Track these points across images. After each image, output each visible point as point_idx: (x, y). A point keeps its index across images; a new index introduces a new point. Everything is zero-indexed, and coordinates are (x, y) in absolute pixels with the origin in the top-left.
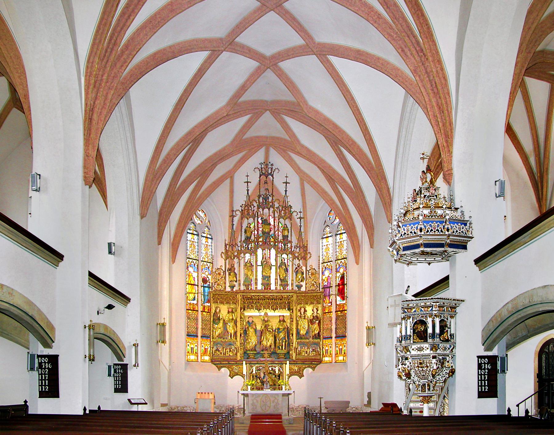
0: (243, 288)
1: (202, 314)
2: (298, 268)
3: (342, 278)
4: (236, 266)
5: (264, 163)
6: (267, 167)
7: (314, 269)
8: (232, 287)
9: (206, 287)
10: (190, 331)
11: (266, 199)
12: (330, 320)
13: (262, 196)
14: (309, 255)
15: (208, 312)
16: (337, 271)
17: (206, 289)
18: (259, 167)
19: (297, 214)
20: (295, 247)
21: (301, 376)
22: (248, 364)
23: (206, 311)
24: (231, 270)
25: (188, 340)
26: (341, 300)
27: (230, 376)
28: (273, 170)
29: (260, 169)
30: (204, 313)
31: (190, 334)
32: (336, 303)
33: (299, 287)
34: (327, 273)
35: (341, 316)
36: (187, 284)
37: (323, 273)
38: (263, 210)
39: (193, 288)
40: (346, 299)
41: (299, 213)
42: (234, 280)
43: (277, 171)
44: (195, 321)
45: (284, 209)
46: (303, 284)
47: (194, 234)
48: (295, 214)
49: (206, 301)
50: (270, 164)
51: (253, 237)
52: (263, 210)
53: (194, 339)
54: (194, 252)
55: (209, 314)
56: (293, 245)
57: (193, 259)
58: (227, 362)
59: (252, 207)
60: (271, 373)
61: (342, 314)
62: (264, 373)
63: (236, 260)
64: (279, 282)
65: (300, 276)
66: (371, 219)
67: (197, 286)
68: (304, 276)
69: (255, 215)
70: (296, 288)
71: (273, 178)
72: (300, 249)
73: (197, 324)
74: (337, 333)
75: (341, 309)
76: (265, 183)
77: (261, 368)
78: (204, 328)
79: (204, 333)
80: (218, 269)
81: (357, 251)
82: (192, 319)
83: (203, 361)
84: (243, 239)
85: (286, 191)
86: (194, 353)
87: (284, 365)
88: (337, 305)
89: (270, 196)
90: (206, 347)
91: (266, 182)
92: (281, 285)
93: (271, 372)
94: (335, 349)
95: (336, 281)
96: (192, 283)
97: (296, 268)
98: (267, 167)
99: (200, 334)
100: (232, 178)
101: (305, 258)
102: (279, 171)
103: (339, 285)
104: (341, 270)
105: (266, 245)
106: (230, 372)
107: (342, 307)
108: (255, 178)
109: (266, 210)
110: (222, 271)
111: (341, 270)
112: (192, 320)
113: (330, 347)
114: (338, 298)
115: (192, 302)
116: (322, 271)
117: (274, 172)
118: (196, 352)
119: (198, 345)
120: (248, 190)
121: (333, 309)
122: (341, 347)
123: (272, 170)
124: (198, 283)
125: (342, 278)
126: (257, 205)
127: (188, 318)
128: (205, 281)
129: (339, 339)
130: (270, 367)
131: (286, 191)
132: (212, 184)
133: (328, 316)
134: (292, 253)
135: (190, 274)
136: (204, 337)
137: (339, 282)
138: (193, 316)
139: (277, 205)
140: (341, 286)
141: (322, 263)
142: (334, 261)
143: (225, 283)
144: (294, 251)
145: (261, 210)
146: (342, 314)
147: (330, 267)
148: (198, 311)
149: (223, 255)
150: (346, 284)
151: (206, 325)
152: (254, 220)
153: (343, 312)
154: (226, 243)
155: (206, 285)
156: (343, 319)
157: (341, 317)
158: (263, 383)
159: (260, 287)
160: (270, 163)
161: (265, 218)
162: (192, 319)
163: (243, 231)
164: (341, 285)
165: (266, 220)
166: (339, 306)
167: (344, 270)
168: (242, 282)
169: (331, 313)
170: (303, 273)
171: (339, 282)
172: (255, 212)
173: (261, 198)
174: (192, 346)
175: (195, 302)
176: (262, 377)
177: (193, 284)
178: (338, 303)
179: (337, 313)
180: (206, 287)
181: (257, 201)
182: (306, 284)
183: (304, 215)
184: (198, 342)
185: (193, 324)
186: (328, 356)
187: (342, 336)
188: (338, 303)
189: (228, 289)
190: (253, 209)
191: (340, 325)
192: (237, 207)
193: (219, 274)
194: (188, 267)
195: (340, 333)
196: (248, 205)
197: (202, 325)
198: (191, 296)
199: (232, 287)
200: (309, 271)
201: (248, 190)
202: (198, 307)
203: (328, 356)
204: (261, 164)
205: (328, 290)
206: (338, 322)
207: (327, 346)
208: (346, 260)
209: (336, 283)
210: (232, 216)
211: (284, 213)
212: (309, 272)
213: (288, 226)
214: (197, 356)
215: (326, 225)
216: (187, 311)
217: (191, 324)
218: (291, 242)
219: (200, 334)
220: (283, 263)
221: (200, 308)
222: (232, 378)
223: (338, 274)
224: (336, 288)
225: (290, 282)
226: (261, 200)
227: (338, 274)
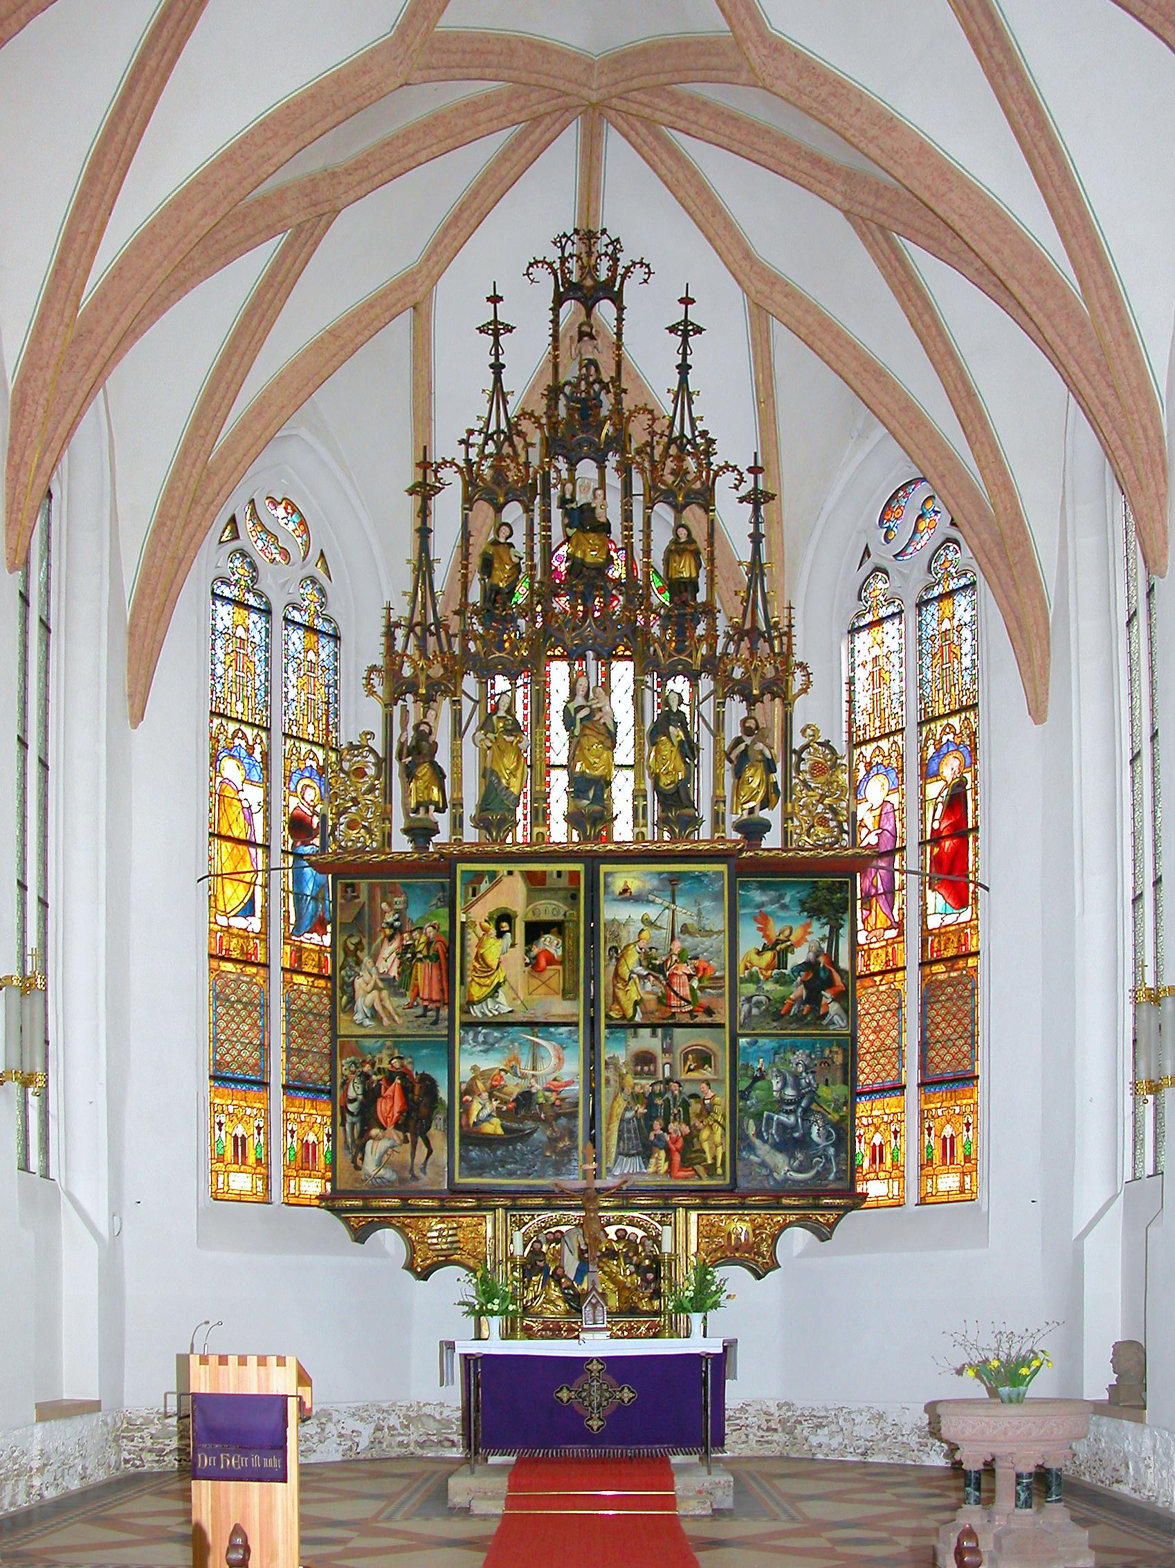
1: (288, 983)
3: (956, 801)
5: (576, 231)
6: (589, 254)
7: (826, 744)
10: (228, 1058)
11: (586, 409)
12: (894, 1006)
14: (799, 676)
16: (928, 773)
18: (554, 255)
19: (741, 481)
22: (500, 1211)
23: (306, 969)
25: (217, 1101)
26: (950, 910)
28: (621, 271)
32: (925, 922)
34: (876, 790)
35: (950, 982)
36: (211, 834)
38: (572, 468)
39: (243, 858)
40: (976, 899)
41: (749, 477)
42: (431, 802)
46: (773, 815)
47: (248, 607)
48: (724, 484)
49: (306, 922)
50: (605, 240)
51: (521, 595)
52: (572, 468)
53: (250, 1095)
54: (250, 692)
57: (241, 721)
58: (396, 1202)
60: (612, 1254)
61: (954, 974)
62: (581, 1252)
64: (653, 808)
65: (755, 779)
66: (1044, 610)
67: (260, 851)
69: (534, 485)
71: (621, 309)
72: (753, 643)
73: (265, 1029)
74: (932, 1067)
76: (582, 335)
77: (564, 1229)
78: (299, 1049)
79: (300, 1073)
81: (1037, 656)
82: (239, 1001)
83: (292, 1201)
85: (684, 368)
86: (251, 1159)
87: (681, 1211)
88: (930, 932)
89: (605, 387)
90: (311, 1138)
91: (586, 329)
93: (616, 1246)
94: (921, 1140)
95: (923, 820)
96: (237, 832)
98: (589, 254)
99: (278, 1077)
100: (421, 310)
101: (778, 688)
102: (649, 273)
103: (937, 837)
104: (950, 768)
106: (412, 1250)
109: (587, 469)
110: (371, 758)
111: (950, 768)
112: (240, 1007)
113: (896, 1132)
114: (936, 900)
115: (239, 922)
118: (258, 1161)
119: (267, 1120)
120: (497, 368)
121: (910, 954)
122: (948, 1131)
124: (267, 836)
125: (956, 801)
127: (217, 997)
128: (299, 826)
129: (940, 1093)
130: (609, 1224)
131: (684, 368)
132: (322, 339)
133: (881, 988)
134: (713, 665)
135: (229, 792)
136: (299, 1089)
137: (936, 825)
138: (244, 987)
139: (638, 432)
142: (912, 730)
143: (386, 817)
145: (562, 464)
146: (954, 974)
147: (893, 761)
148: (266, 966)
149: (376, 681)
150: (976, 829)
151: (306, 1033)
152: (528, 510)
153: (961, 963)
156: (960, 996)
157: (950, 990)
158: (575, 1301)
160: (604, 232)
161: (581, 499)
162: (239, 1001)
163: (475, 562)
164: (947, 837)
165: (587, 510)
166: (939, 935)
167: (963, 767)
169: (900, 975)
171: (936, 825)
173: (562, 402)
174: (240, 1131)
175: (255, 924)
176: (572, 1275)
177: (242, 836)
178: (933, 922)
179: (927, 971)
182: (787, 817)
184: (268, 1111)
186: (882, 1175)
187: (953, 1081)
188: (933, 922)
190: (522, 459)
191: (943, 1025)
192: (446, 447)
194: (215, 760)
195: (944, 1062)
197: (287, 1034)
198: (234, 895)
200: (799, 753)
201: (497, 368)
202: (268, 949)
203: (882, 1175)
207: (877, 1129)
208: (971, 715)
209: (923, 831)
210: (424, 491)
211: (673, 473)
213: (694, 535)
214: (267, 1178)
215: (869, 565)
216: (214, 964)
217: (234, 1026)
219: (278, 1077)
221: (281, 956)
223: (933, 789)
224: (923, 853)
225: (705, 811)
227: (933, 789)
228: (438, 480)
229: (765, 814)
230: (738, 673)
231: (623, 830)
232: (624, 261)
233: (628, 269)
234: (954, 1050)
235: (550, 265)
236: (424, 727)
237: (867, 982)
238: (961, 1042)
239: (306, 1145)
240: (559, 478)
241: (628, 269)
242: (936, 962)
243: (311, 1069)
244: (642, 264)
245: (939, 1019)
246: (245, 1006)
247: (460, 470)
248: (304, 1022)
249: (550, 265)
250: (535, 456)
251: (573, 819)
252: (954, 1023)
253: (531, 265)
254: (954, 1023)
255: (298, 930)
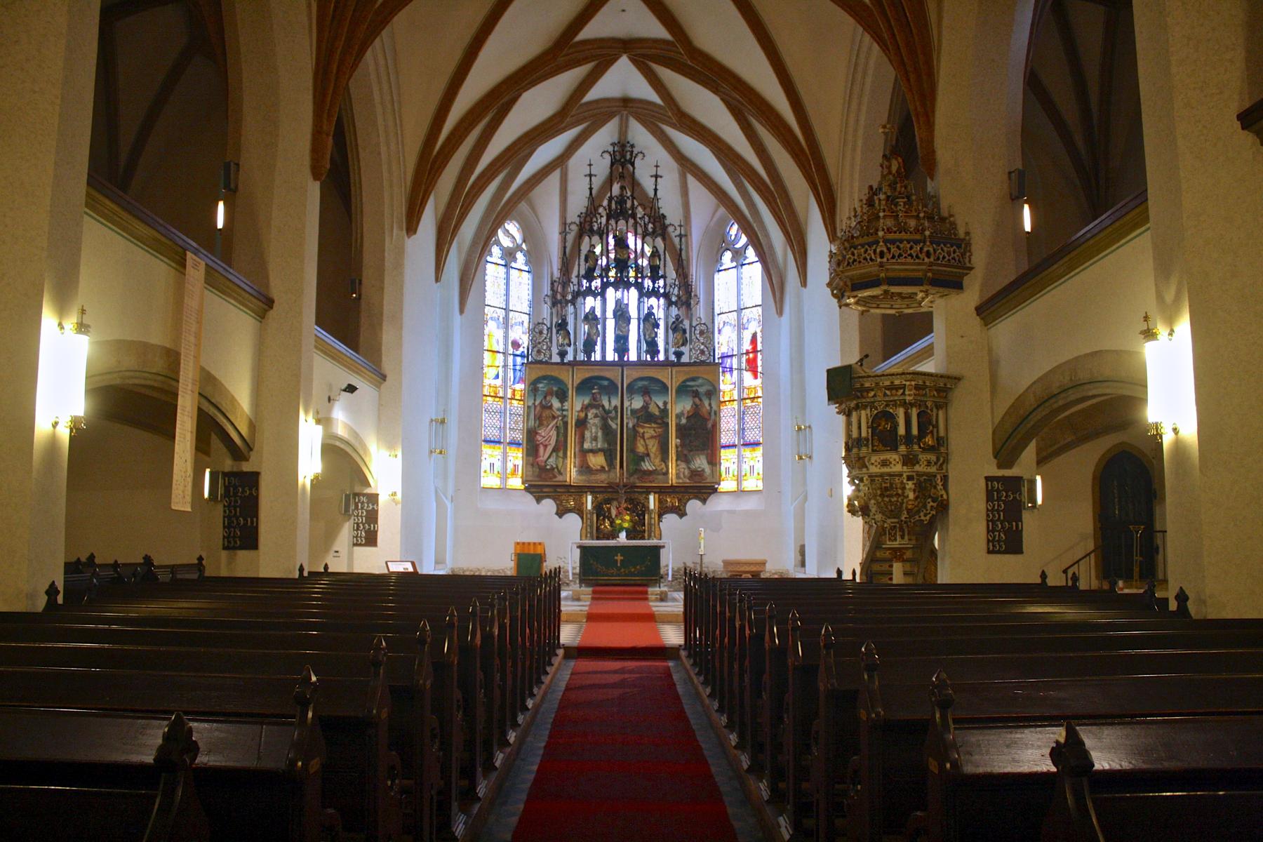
0: (581, 357)
2: (677, 322)
4: (570, 320)
5: (619, 142)
6: (623, 151)
7: (704, 324)
8: (563, 354)
9: (518, 356)
10: (489, 433)
12: (733, 414)
13: (615, 198)
15: (520, 400)
17: (519, 360)
20: (671, 286)
21: (682, 514)
23: (516, 398)
24: (562, 326)
27: (557, 514)
28: (634, 155)
29: (612, 153)
30: (514, 401)
31: (488, 439)
33: (679, 355)
37: (720, 331)
38: (616, 223)
43: (640, 156)
44: (498, 416)
45: (652, 220)
46: (685, 349)
48: (670, 229)
49: (517, 379)
50: (629, 145)
52: (616, 223)
55: (522, 403)
56: (669, 281)
59: (598, 216)
63: (570, 309)
68: (688, 335)
69: (603, 231)
70: (673, 358)
71: (634, 168)
74: (746, 438)
75: (752, 396)
78: (514, 429)
80: (539, 323)
84: (583, 272)
85: (656, 190)
86: (496, 472)
92: (647, 352)
97: (674, 322)
101: (688, 305)
102: (644, 156)
105: (623, 283)
107: (753, 390)
108: (603, 167)
109: (622, 223)
110: (545, 327)
112: (493, 413)
116: (718, 328)
117: (635, 157)
118: (498, 472)
123: (631, 155)
126: (607, 214)
131: (656, 190)
140: (751, 355)
141: (718, 314)
144: (669, 292)
145: (612, 222)
149: (547, 299)
151: (516, 422)
152: (601, 238)
153: (756, 400)
154: (554, 279)
155: (518, 353)
157: (752, 410)
159: (611, 356)
160: (628, 142)
164: (751, 352)
166: (748, 389)
168: (580, 346)
170: (684, 331)
172: (603, 226)
173: (613, 203)
178: (746, 384)
180: (518, 356)
181: (607, 207)
182: (691, 350)
183: (686, 230)
185: (495, 421)
186: (729, 479)
189: (556, 359)
191: (750, 423)
192: (573, 215)
193: (541, 333)
196: (591, 213)
199: (563, 354)
201: (591, 189)
204: (613, 144)
205: (729, 360)
206: (746, 418)
212: (695, 330)
217: (491, 421)
218: (664, 277)
220: (650, 314)
222: (560, 517)
225: (661, 347)
226: (613, 206)
228: (570, 229)
229: (683, 349)
230: (674, 299)
231: (633, 356)
232: (635, 152)
233: (637, 155)
234: (753, 433)
235: (610, 153)
236: (564, 317)
237: (724, 404)
238: (755, 430)
239: (515, 466)
240: (612, 229)
241: (637, 155)
242: (748, 399)
243: (517, 436)
244: (641, 153)
245: (748, 420)
246: (495, 413)
247: (577, 225)
248: (515, 418)
249: (610, 153)
250: (604, 220)
251: (615, 350)
252: (754, 422)
253: (603, 153)
254: (754, 422)
255: (514, 383)
